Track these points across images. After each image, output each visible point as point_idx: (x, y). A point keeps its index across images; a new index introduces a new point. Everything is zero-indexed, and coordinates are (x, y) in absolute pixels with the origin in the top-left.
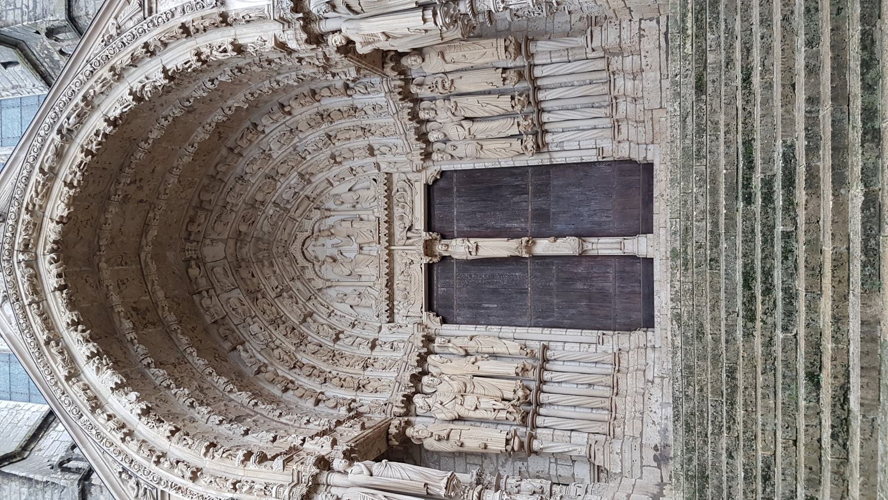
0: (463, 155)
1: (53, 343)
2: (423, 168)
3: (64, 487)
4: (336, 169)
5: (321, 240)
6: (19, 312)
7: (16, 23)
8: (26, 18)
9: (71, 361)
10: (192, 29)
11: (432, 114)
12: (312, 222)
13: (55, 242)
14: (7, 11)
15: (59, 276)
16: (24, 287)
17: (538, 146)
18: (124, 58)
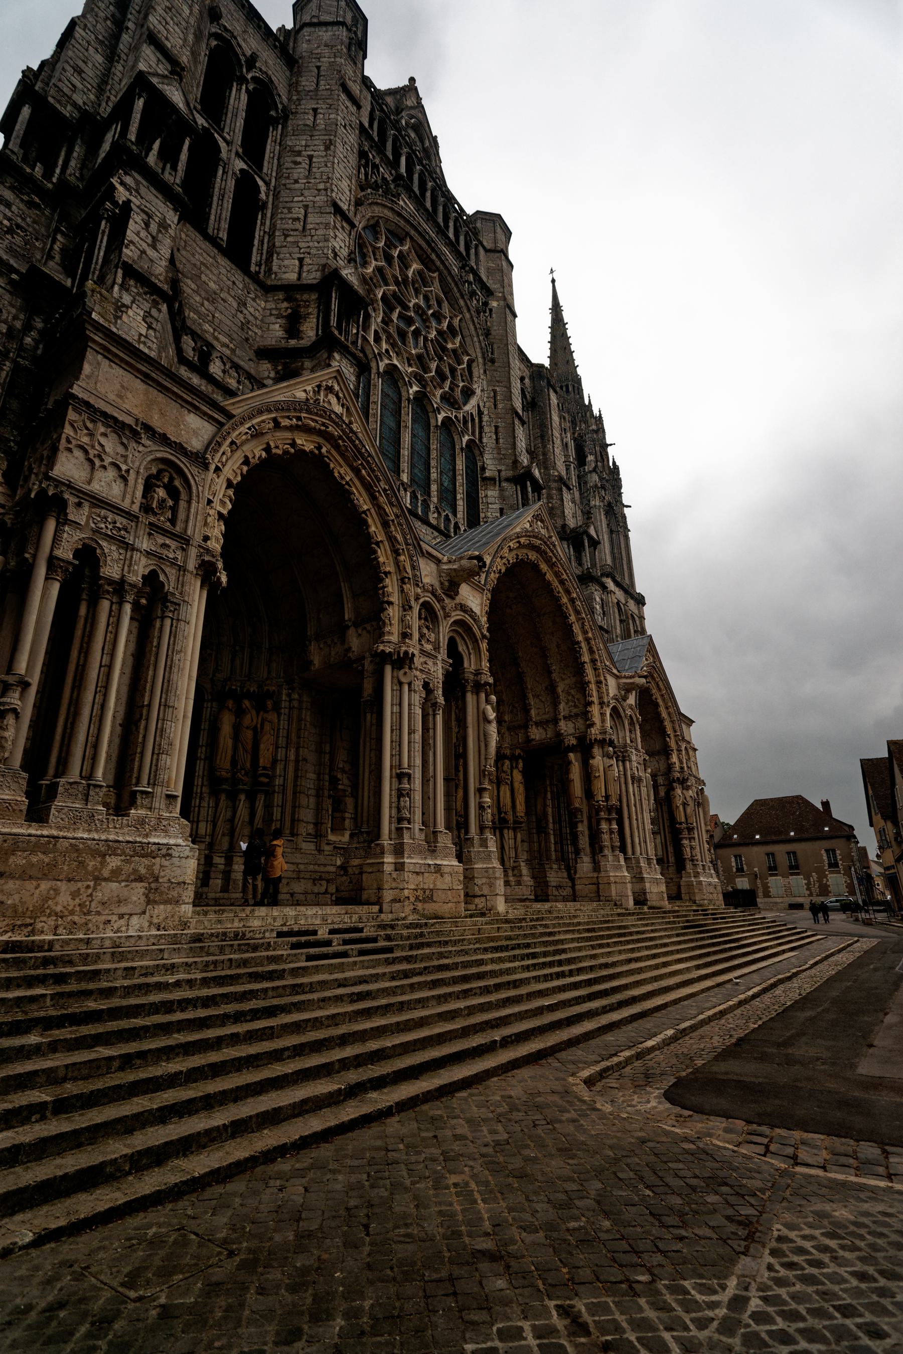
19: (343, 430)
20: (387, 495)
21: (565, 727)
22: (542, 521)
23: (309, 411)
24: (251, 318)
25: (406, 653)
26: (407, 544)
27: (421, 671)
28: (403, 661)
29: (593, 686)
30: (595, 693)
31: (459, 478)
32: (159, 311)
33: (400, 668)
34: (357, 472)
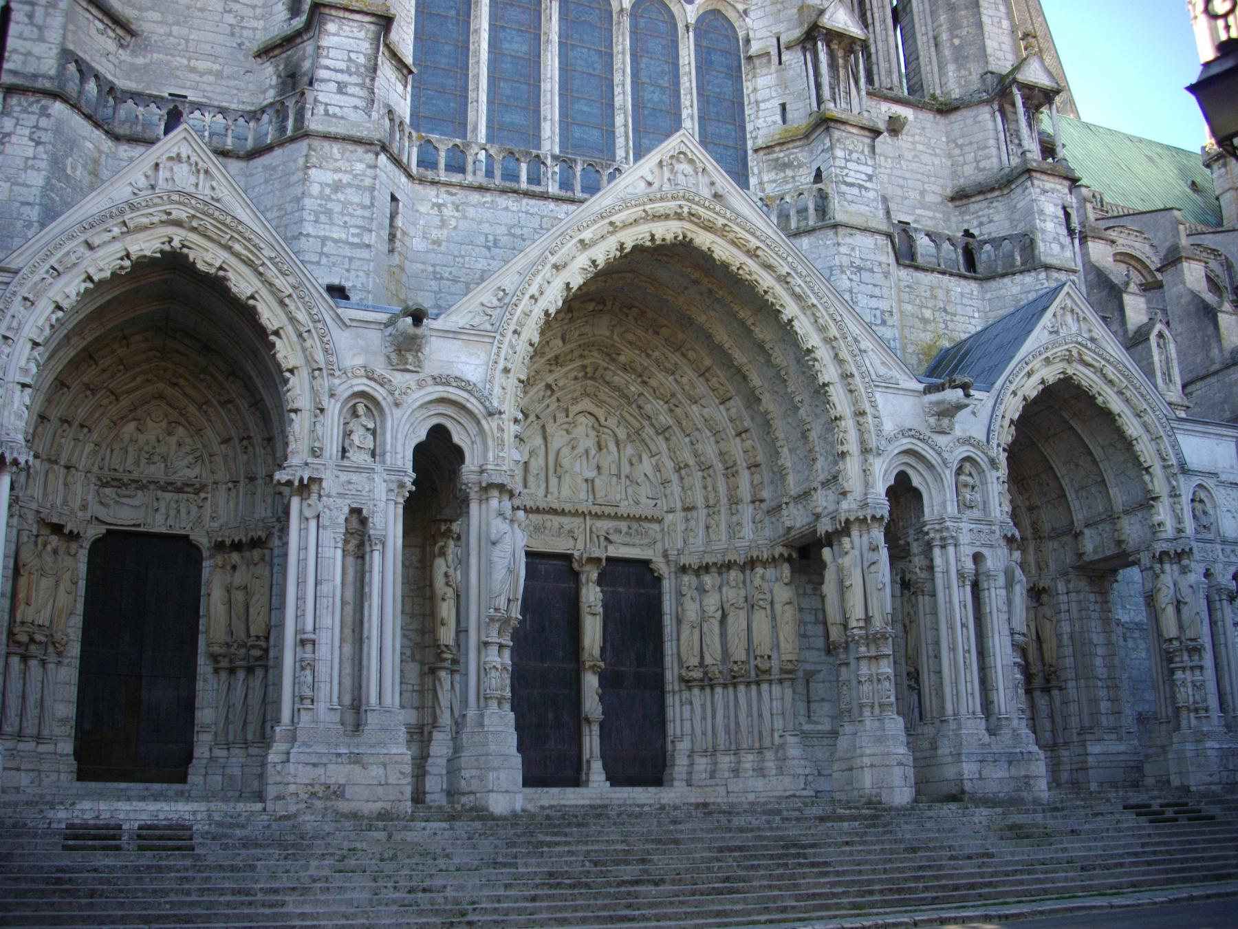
0: (686, 606)
1: (611, 229)
2: (668, 562)
3: (370, 116)
4: (670, 465)
5: (593, 434)
6: (641, 201)
7: (834, 158)
8: (838, 171)
9: (594, 243)
10: (861, 420)
11: (733, 583)
12: (614, 427)
13: (691, 240)
14: (844, 149)
15: (664, 240)
16: (659, 207)
17: (689, 681)
18: (844, 354)
19: (193, 208)
20: (275, 265)
21: (823, 500)
22: (691, 161)
23: (133, 207)
24: (247, 12)
25: (301, 480)
26: (315, 322)
27: (341, 495)
28: (304, 488)
29: (849, 423)
30: (852, 436)
31: (684, 81)
32: (49, 116)
33: (309, 498)
34: (229, 249)
